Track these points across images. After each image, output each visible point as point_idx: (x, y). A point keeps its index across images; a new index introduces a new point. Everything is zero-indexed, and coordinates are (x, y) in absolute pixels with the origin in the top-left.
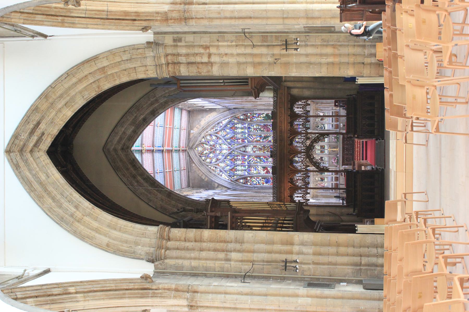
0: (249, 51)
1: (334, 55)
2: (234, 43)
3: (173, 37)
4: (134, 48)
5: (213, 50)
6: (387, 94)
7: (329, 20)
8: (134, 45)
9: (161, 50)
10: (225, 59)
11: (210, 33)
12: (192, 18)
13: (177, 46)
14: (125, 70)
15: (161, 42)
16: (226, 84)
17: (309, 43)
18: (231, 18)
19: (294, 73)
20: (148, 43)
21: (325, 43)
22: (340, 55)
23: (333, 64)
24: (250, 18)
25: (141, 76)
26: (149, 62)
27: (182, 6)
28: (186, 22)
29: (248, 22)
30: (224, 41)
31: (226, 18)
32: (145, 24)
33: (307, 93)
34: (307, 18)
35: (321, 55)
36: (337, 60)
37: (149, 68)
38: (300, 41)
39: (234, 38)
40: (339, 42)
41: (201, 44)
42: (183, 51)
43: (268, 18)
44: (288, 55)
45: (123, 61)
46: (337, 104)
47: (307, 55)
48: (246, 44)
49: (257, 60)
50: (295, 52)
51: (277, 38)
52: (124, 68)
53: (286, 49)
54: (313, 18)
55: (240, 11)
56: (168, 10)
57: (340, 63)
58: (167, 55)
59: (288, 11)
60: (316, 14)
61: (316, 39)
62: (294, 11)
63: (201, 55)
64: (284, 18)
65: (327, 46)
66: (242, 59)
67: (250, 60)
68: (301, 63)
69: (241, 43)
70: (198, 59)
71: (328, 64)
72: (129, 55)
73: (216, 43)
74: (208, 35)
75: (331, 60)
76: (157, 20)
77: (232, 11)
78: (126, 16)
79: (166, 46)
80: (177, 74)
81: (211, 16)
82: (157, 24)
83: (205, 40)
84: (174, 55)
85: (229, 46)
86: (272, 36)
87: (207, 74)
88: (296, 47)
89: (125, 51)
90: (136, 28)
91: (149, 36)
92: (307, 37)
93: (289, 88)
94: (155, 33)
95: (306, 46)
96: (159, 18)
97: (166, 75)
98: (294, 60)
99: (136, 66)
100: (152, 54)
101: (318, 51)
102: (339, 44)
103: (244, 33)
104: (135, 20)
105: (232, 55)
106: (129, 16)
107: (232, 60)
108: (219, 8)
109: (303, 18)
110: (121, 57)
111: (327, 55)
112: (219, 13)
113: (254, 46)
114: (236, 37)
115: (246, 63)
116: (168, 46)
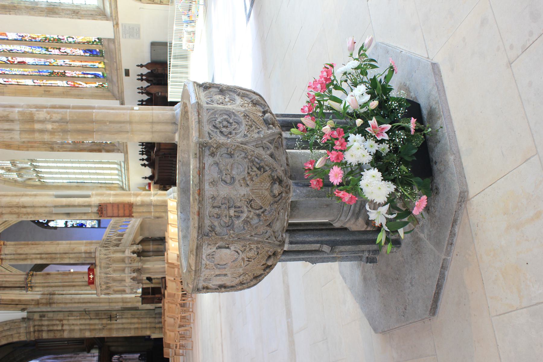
0: (88, 322)
1: (138, 323)
2: (78, 318)
3: (40, 315)
4: (13, 322)
5: (65, 322)
6: (164, 339)
7: (135, 303)
8: (13, 320)
9: (31, 323)
10: (72, 327)
11: (64, 311)
12: (54, 303)
13: (41, 320)
14: (5, 336)
15: (31, 318)
16: (70, 344)
17: (124, 317)
18: (78, 303)
19: (115, 334)
20: (23, 319)
21: (133, 316)
22: (142, 323)
23: (138, 328)
24: (90, 302)
25: (16, 340)
26: (22, 330)
27: (48, 296)
28: (50, 306)
29: (89, 305)
30: (72, 316)
31: (75, 303)
32: (23, 307)
33: (120, 349)
34: (123, 302)
35: (131, 323)
36: (140, 326)
37: (21, 334)
38: (119, 315)
39: (79, 315)
40: (141, 315)
41: (58, 318)
42: (46, 323)
43: (100, 303)
44: (111, 324)
45: (4, 330)
46: (140, 358)
47: (122, 324)
48: (86, 318)
49: (92, 327)
50: (115, 322)
51: (105, 314)
52: (4, 335)
53: (111, 320)
54: (126, 302)
55: (84, 299)
56: (40, 299)
57: (142, 328)
58: (34, 326)
59: (112, 299)
60: (128, 300)
61: (128, 314)
62: (116, 298)
63: (57, 325)
64: (109, 303)
65: (134, 318)
66: (83, 327)
67: (88, 327)
68: (119, 329)
69: (83, 317)
70: (55, 328)
71: (135, 328)
72: (9, 326)
73: (67, 318)
74: (62, 313)
75: (136, 326)
76: (31, 305)
77: (79, 299)
78: (12, 302)
79: (34, 320)
80: (40, 338)
81: (66, 301)
82: (32, 306)
83: (60, 316)
84: (39, 325)
85: (75, 319)
86: (102, 313)
87: (60, 337)
88: (116, 319)
89: (6, 324)
90: (17, 309)
91: (24, 314)
92: (123, 313)
93: (109, 346)
94: (28, 312)
95: (122, 318)
96: (33, 303)
97: (33, 339)
98: (115, 326)
99: (13, 333)
100: (25, 325)
101: (129, 321)
102: (141, 316)
103: (85, 311)
104: (17, 304)
105: (77, 325)
106: (14, 302)
107: (76, 328)
108: (71, 297)
109: (120, 302)
110: (3, 328)
111: (134, 323)
112: (71, 300)
113: (91, 319)
114: (80, 314)
115: (85, 329)
116: (36, 320)
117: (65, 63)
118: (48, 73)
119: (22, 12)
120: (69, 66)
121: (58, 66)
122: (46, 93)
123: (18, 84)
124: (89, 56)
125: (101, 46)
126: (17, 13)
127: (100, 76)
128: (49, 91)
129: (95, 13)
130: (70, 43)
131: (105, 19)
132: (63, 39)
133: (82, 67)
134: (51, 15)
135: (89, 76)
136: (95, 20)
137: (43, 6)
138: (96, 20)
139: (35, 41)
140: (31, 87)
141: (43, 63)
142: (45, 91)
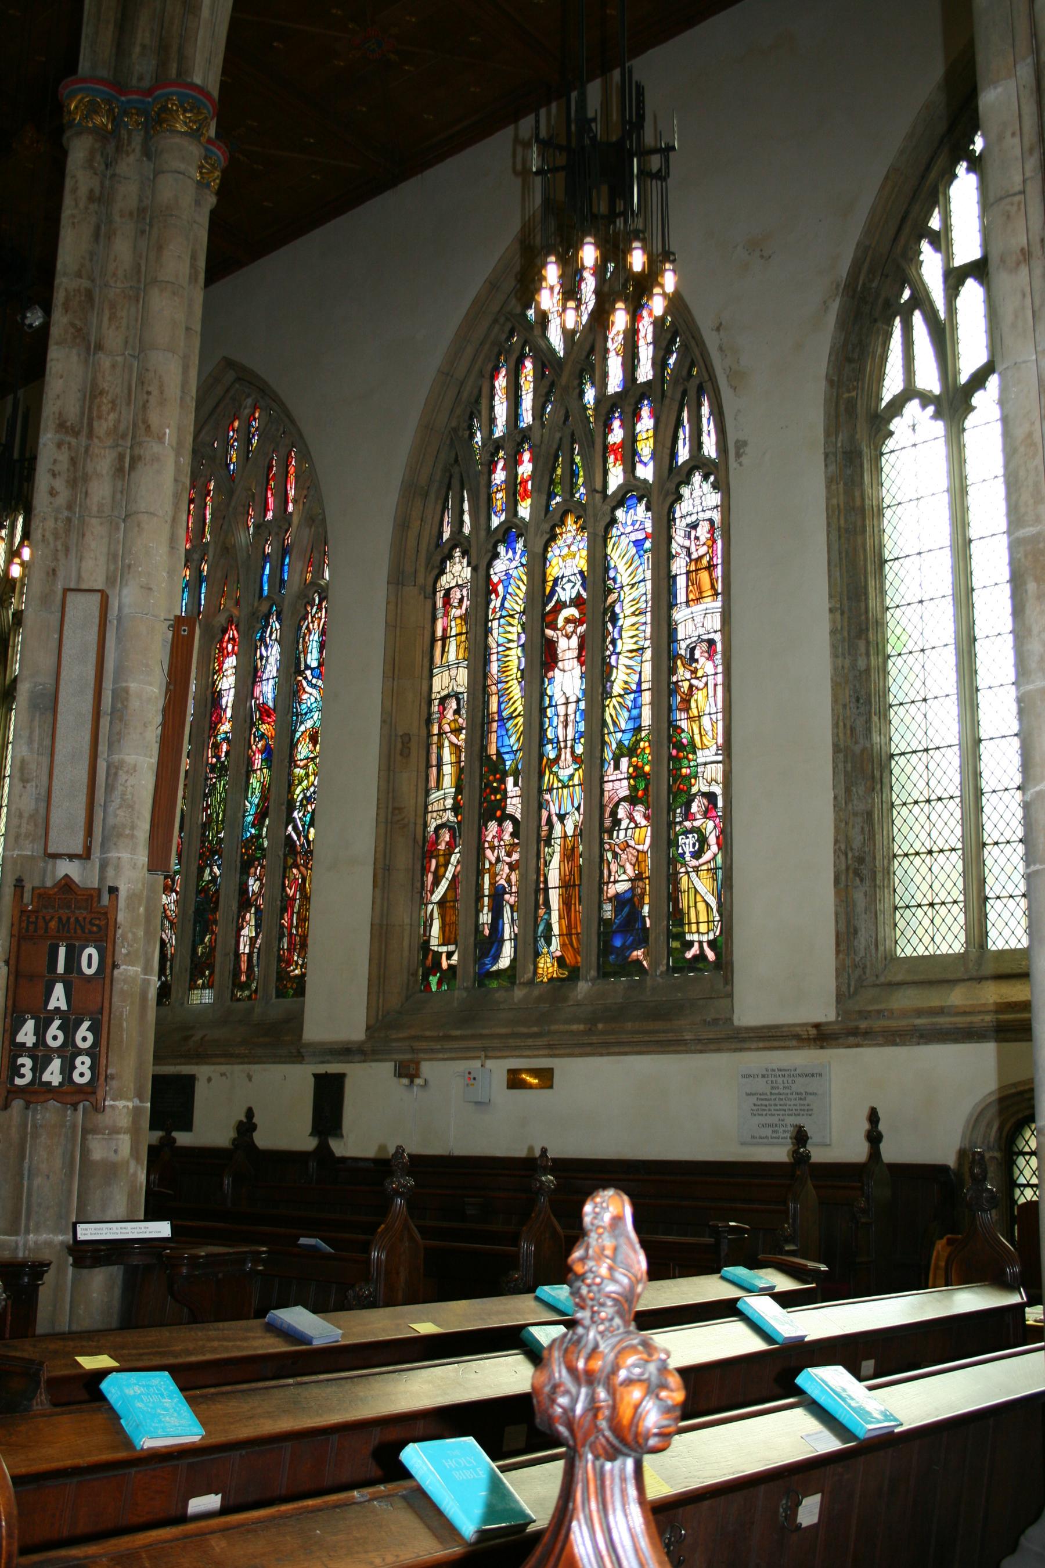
117: (555, 819)
118: (499, 754)
119: (843, 654)
120: (539, 835)
121: (540, 791)
122: (399, 740)
123: (433, 640)
124: (601, 920)
125: (663, 968)
126: (839, 636)
127: (487, 960)
128: (405, 752)
129: (862, 947)
130: (673, 843)
131: (844, 989)
132: (688, 816)
133: (537, 891)
134: (841, 766)
135: (486, 917)
136: (838, 945)
137: (876, 738)
138: (838, 952)
139: (670, 707)
140: (425, 688)
141: (550, 734)
142: (406, 739)
